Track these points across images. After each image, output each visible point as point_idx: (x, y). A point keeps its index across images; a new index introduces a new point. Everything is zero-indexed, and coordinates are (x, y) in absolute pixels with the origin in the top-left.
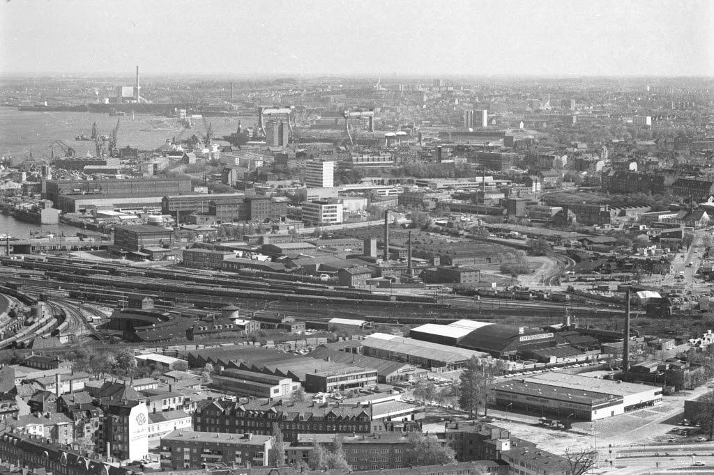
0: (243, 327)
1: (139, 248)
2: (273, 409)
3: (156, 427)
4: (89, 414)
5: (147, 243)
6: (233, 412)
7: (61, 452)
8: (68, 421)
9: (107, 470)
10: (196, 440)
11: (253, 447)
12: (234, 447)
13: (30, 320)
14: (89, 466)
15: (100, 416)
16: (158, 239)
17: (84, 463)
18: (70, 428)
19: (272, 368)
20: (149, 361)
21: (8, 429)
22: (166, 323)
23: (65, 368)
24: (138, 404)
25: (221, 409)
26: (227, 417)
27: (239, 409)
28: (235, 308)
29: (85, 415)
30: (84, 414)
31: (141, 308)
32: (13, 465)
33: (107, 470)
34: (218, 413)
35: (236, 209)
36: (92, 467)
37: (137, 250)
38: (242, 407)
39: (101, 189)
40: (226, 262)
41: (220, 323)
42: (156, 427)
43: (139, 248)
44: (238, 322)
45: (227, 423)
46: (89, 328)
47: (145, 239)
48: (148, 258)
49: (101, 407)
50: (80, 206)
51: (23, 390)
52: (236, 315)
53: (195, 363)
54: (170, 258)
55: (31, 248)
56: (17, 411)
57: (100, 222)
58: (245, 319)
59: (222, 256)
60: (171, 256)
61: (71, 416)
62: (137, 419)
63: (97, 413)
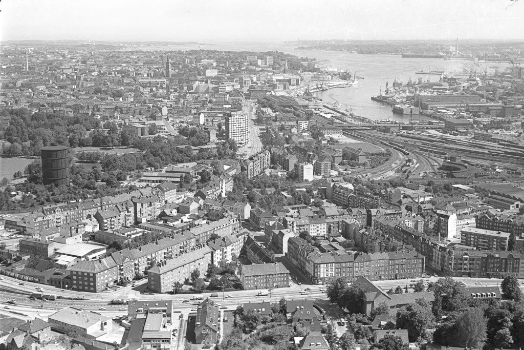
0: (500, 173)
2: (512, 220)
3: (459, 222)
4: (431, 217)
6: (494, 220)
7: (419, 237)
8: (423, 219)
10: (477, 232)
11: (502, 238)
12: (494, 237)
13: (408, 164)
17: (429, 243)
18: (423, 223)
19: (512, 196)
20: (458, 188)
21: (398, 223)
22: (466, 170)
23: (421, 191)
26: (491, 222)
27: (497, 219)
32: (399, 243)
34: (487, 220)
37: (454, 130)
38: (498, 218)
42: (459, 222)
44: (498, 170)
45: (491, 224)
46: (433, 169)
51: (404, 201)
52: (497, 167)
53: (477, 190)
56: (401, 213)
58: (500, 169)
61: (424, 218)
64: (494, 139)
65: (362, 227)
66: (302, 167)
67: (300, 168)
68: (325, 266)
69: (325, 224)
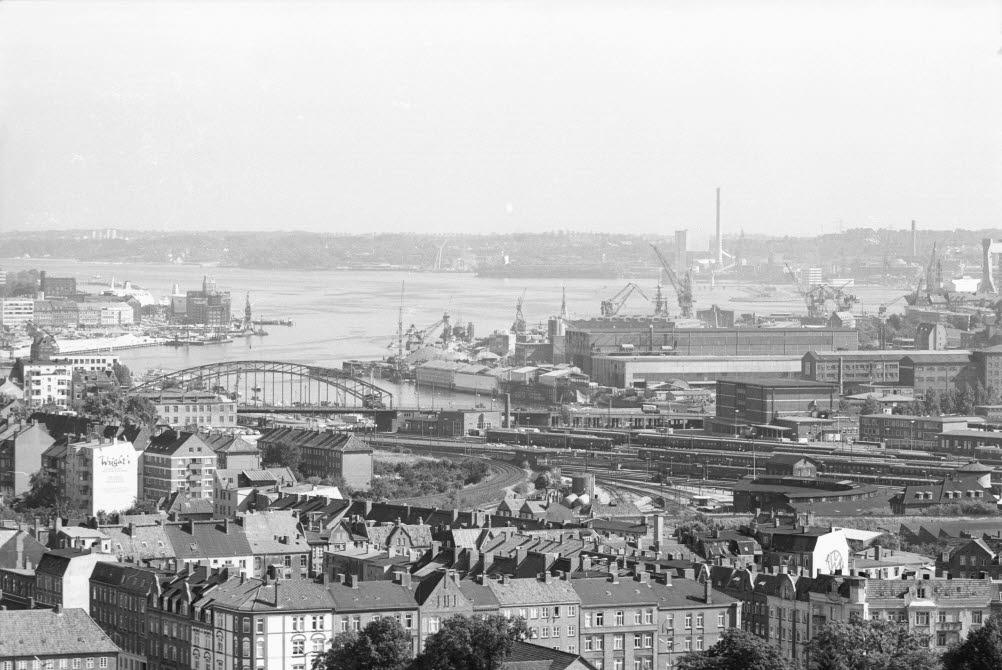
1: (769, 418)
5: (783, 406)
9: (794, 583)
14: (756, 582)
15: (756, 553)
16: (806, 399)
24: (830, 531)
25: (991, 553)
28: (984, 468)
29: (726, 550)
30: (725, 547)
31: (791, 474)
33: (794, 583)
35: (954, 374)
36: (763, 583)
37: (764, 422)
39: (675, 345)
40: (947, 437)
41: (957, 486)
43: (769, 418)
47: (779, 400)
48: (787, 434)
49: (758, 537)
50: (636, 375)
54: (831, 435)
55: (550, 420)
57: (679, 399)
59: (940, 424)
60: (835, 432)
62: (827, 560)
63: (750, 546)
64: (951, 438)
65: (426, 559)
66: (86, 459)
67: (72, 465)
68: (289, 628)
69: (250, 560)
